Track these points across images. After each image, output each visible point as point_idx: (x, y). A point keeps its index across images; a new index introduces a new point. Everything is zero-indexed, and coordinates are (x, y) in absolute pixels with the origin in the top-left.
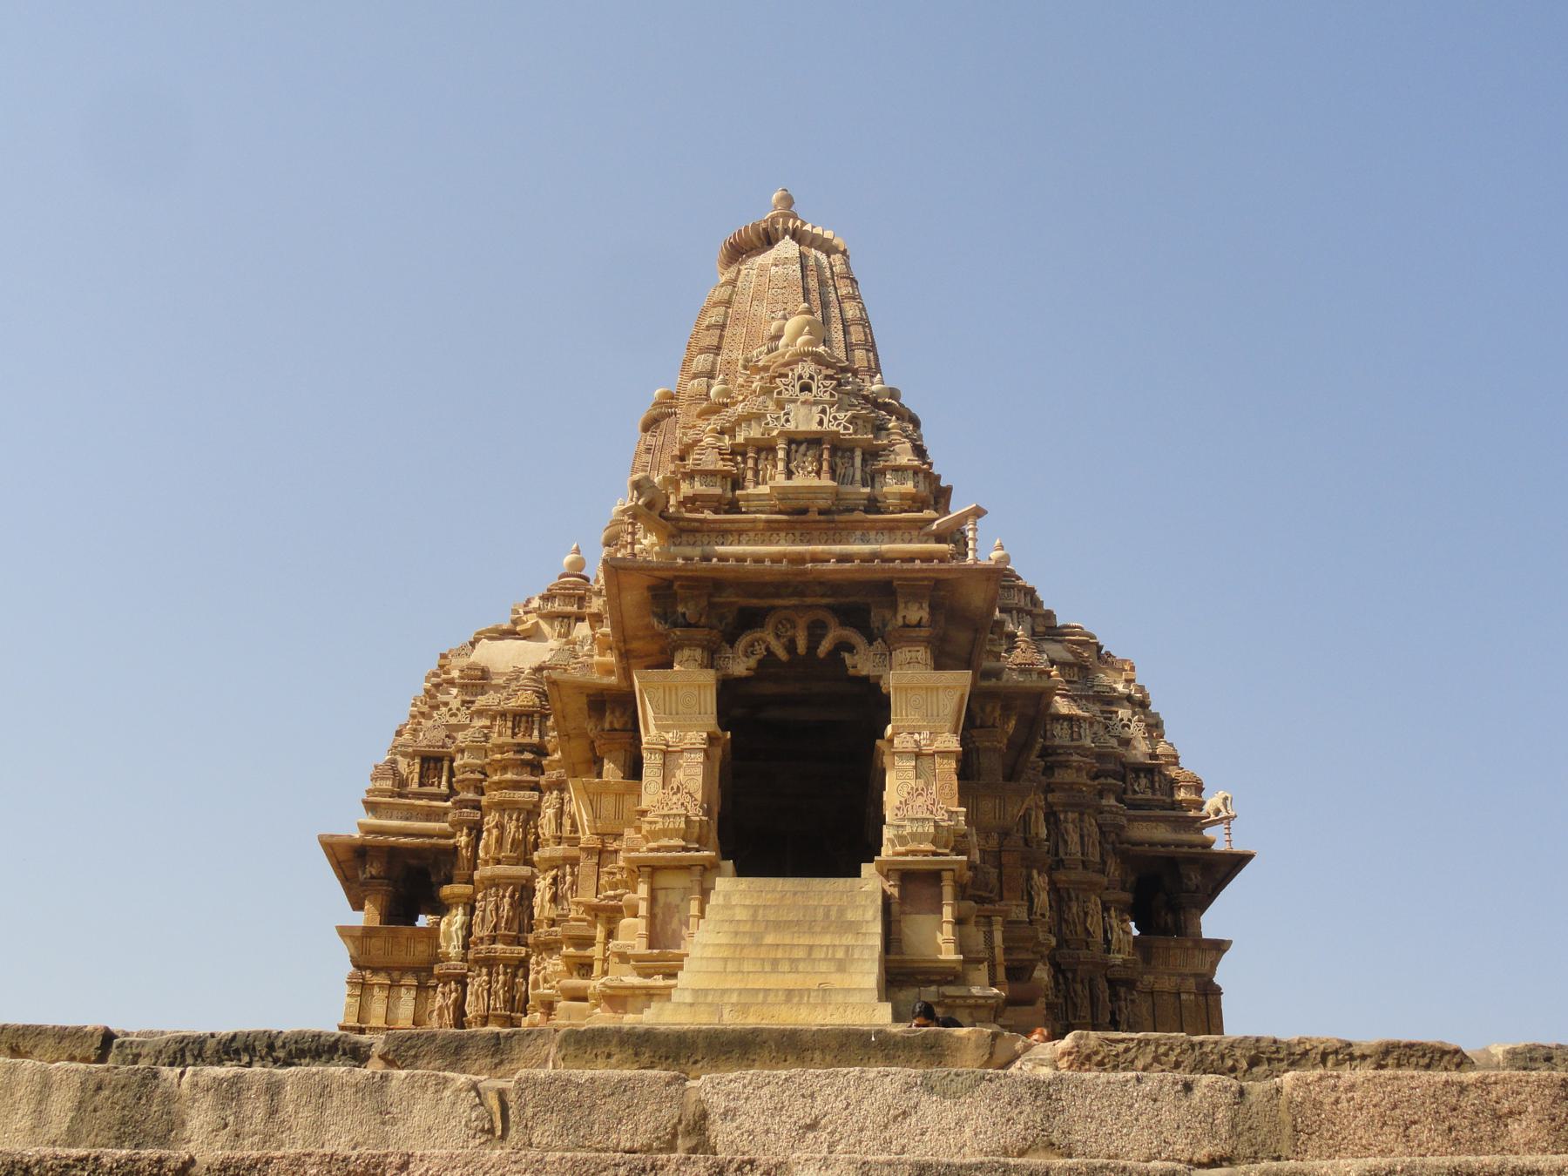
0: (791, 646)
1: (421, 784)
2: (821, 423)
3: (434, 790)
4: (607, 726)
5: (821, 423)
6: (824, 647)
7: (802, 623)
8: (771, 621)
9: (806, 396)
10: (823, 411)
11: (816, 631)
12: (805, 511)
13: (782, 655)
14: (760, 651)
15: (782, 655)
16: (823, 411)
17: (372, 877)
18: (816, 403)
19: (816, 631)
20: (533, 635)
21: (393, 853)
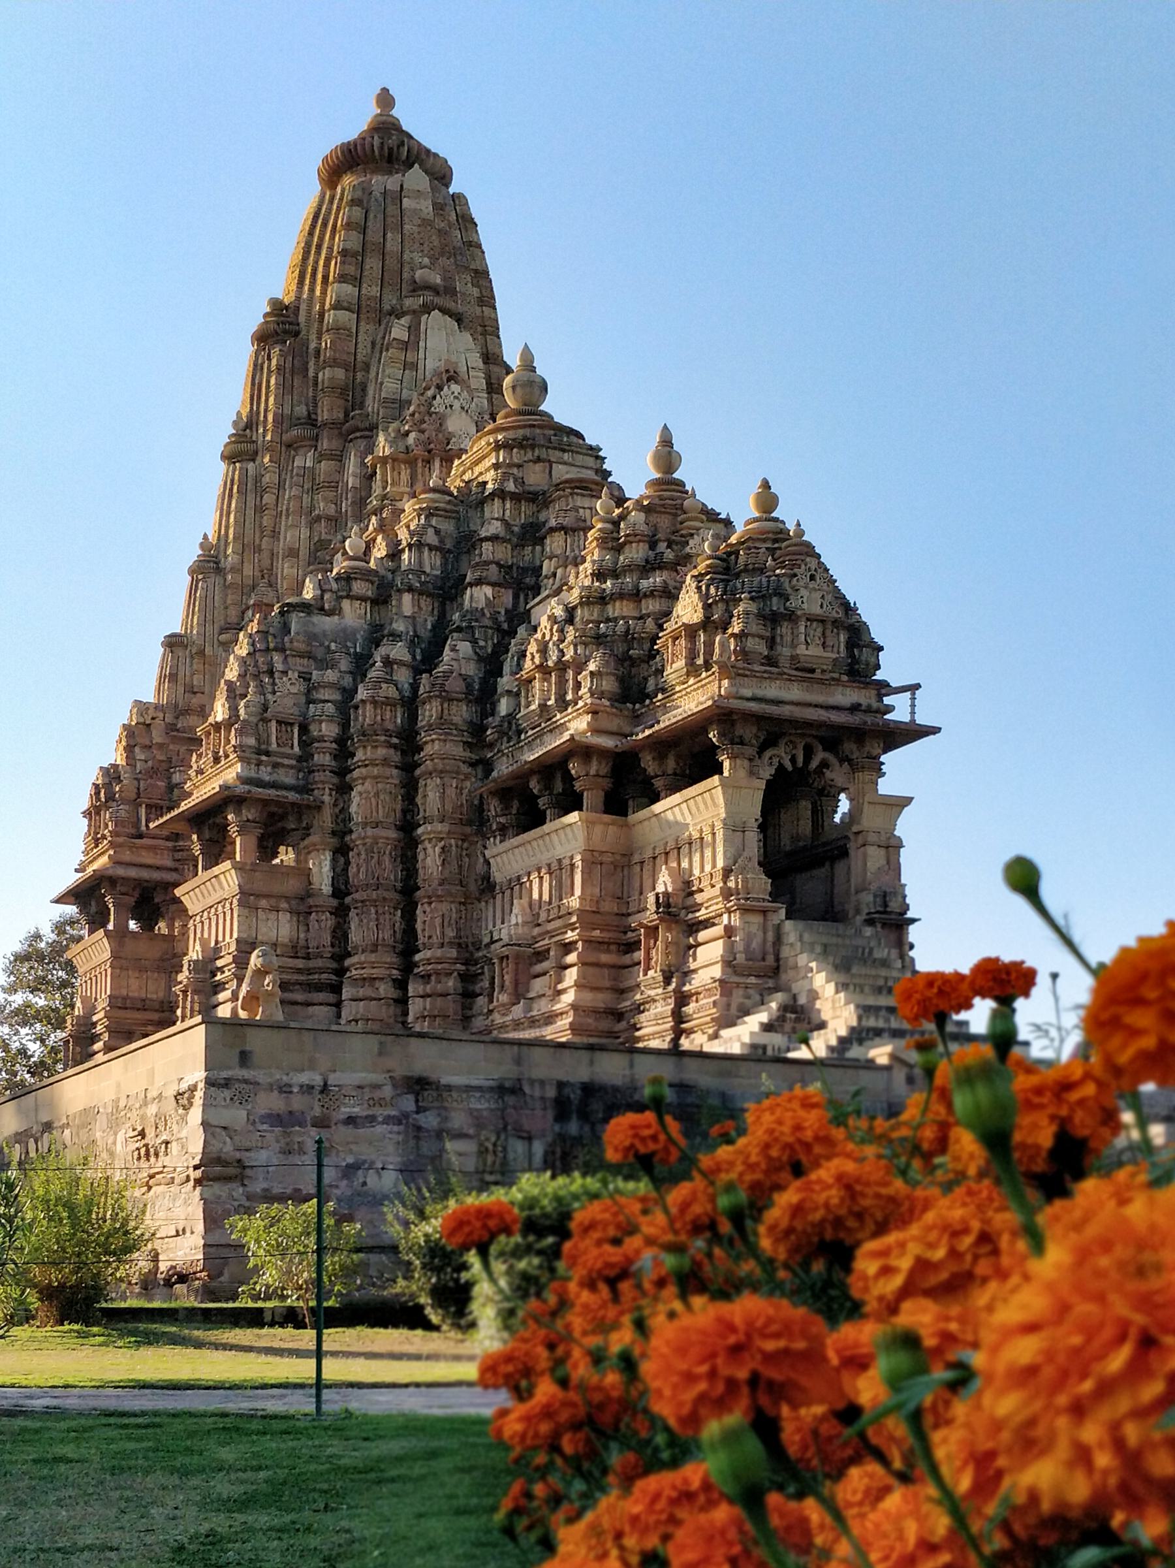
0: (793, 760)
1: (278, 745)
2: (822, 606)
3: (287, 750)
4: (592, 772)
5: (822, 606)
6: (814, 764)
7: (801, 747)
8: (782, 743)
9: (812, 585)
11: (809, 753)
12: (812, 671)
13: (789, 766)
14: (776, 761)
15: (789, 766)
17: (248, 820)
19: (809, 753)
20: (335, 611)
21: (265, 803)
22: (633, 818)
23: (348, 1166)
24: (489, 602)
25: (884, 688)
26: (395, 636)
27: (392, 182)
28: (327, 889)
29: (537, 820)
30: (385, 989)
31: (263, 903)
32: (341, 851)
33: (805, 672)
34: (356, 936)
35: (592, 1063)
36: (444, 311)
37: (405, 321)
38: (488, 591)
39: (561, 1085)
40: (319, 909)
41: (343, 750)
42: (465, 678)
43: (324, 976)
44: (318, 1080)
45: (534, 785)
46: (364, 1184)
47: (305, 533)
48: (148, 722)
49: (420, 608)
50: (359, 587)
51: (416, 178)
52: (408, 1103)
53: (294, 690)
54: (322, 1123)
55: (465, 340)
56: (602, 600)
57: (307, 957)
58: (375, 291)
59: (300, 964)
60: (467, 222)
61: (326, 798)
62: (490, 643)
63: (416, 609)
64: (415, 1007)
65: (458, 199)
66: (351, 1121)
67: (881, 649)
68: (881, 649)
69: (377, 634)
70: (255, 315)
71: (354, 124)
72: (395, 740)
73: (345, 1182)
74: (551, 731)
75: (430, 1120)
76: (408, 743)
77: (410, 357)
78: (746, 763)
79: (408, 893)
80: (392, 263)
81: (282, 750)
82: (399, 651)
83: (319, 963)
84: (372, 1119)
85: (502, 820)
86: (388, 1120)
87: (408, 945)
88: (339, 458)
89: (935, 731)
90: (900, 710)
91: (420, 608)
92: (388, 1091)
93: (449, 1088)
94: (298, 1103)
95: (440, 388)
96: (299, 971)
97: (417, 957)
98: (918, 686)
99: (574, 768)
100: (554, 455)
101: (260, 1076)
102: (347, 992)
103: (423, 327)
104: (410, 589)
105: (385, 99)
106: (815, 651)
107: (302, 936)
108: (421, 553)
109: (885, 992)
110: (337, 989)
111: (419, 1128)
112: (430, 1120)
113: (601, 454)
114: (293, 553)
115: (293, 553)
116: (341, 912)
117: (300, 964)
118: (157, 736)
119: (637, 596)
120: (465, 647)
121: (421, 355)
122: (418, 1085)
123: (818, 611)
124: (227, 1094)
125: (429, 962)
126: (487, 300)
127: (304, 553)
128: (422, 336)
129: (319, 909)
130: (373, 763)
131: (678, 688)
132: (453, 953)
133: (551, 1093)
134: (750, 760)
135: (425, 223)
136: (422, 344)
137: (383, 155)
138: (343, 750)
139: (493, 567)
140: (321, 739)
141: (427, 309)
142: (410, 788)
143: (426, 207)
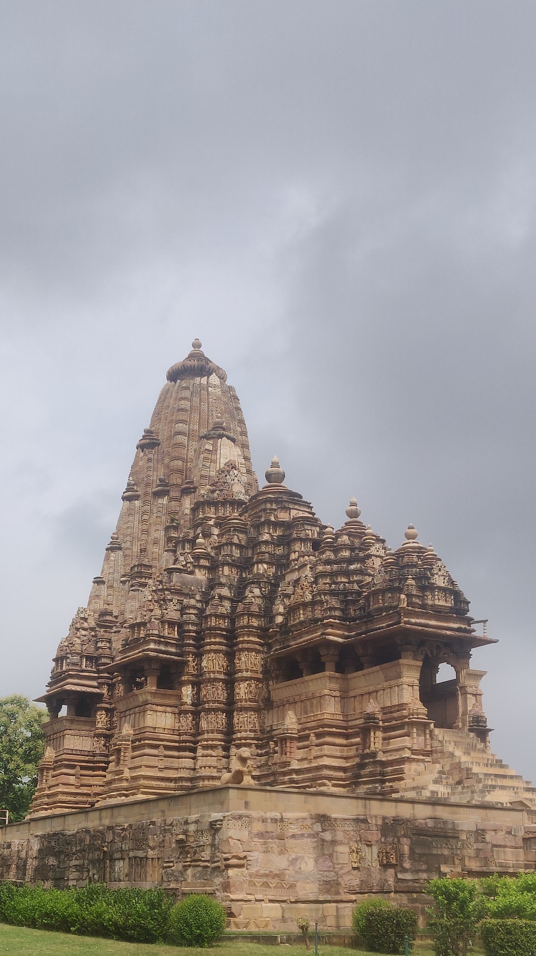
2: (444, 583)
3: (171, 636)
5: (444, 583)
10: (444, 579)
12: (441, 612)
14: (424, 653)
16: (444, 579)
18: (443, 576)
20: (192, 573)
22: (350, 676)
23: (293, 859)
24: (265, 571)
25: (469, 621)
26: (222, 585)
27: (204, 380)
28: (189, 702)
29: (299, 675)
30: (220, 752)
31: (160, 708)
32: (197, 685)
33: (438, 613)
34: (204, 725)
35: (396, 807)
36: (228, 438)
37: (211, 442)
38: (265, 566)
39: (384, 818)
40: (186, 712)
41: (199, 638)
42: (259, 605)
43: (188, 744)
44: (278, 816)
46: (300, 868)
47: (162, 533)
48: (86, 617)
49: (232, 572)
50: (203, 562)
51: (214, 379)
52: (318, 827)
53: (175, 608)
54: (281, 838)
55: (237, 451)
56: (332, 574)
57: (179, 735)
58: (196, 427)
59: (176, 738)
60: (236, 398)
61: (190, 659)
62: (267, 589)
63: (230, 572)
65: (230, 388)
66: (293, 836)
67: (469, 602)
68: (469, 602)
69: (213, 584)
70: (138, 436)
71: (179, 356)
72: (224, 633)
73: (291, 868)
74: (307, 633)
75: (327, 836)
76: (231, 637)
77: (213, 457)
78: (412, 653)
79: (230, 707)
80: (204, 416)
81: (169, 636)
82: (225, 592)
83: (184, 737)
84: (302, 835)
85: (277, 672)
86: (309, 836)
87: (229, 731)
88: (178, 500)
90: (478, 631)
91: (232, 572)
92: (309, 822)
93: (336, 819)
94: (270, 827)
95: (229, 472)
97: (234, 736)
99: (323, 652)
100: (291, 506)
101: (254, 814)
103: (219, 445)
104: (228, 564)
105: (197, 345)
106: (442, 603)
108: (231, 547)
109: (489, 766)
111: (323, 840)
112: (327, 836)
113: (311, 505)
114: (156, 542)
115: (156, 542)
116: (196, 715)
118: (92, 623)
119: (347, 574)
120: (257, 591)
121: (218, 457)
122: (323, 819)
123: (443, 585)
124: (240, 823)
125: (240, 739)
126: (244, 433)
127: (162, 543)
128: (219, 448)
129: (186, 712)
130: (215, 643)
131: (375, 617)
132: (252, 735)
133: (380, 822)
134: (414, 652)
135: (218, 399)
136: (218, 452)
137: (194, 369)
138: (199, 638)
139: (267, 555)
140: (189, 631)
141: (221, 436)
142: (231, 656)
143: (218, 391)
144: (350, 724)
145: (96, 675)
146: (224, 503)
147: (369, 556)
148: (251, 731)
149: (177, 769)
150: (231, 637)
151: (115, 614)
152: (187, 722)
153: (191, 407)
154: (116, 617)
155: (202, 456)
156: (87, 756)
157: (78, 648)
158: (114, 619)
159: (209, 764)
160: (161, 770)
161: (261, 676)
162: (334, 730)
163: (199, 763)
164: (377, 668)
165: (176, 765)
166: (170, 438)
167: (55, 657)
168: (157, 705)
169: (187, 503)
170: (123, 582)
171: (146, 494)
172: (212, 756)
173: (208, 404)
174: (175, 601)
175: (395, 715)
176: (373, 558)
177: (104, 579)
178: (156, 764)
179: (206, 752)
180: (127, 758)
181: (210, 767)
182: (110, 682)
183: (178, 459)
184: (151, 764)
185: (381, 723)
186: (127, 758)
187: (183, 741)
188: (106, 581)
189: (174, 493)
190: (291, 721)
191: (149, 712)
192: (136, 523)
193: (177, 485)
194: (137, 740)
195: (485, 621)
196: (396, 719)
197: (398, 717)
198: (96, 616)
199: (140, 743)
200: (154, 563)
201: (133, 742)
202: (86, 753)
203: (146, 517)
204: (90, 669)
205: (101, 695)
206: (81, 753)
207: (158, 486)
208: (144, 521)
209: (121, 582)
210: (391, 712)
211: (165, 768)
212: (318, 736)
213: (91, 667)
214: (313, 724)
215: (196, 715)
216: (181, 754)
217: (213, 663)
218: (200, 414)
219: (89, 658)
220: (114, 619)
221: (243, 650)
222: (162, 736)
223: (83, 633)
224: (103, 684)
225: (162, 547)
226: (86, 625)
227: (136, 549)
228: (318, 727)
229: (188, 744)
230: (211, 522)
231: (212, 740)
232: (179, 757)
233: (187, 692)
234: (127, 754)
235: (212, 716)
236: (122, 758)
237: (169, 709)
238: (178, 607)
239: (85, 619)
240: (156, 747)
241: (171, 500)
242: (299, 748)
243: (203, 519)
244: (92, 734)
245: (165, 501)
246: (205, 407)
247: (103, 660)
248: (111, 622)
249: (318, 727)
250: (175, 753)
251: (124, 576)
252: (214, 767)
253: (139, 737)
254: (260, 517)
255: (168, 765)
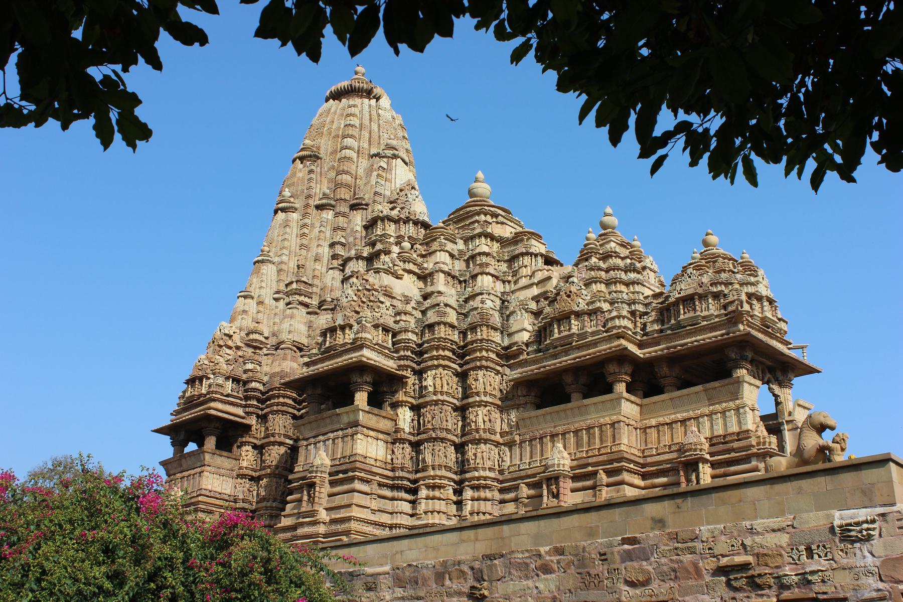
20: (399, 277)
31: (372, 433)
37: (385, 160)
40: (402, 441)
43: (405, 482)
45: (568, 379)
47: (327, 249)
57: (393, 470)
58: (366, 145)
59: (390, 474)
64: (468, 507)
74: (578, 348)
77: (389, 176)
80: (375, 136)
89: (819, 372)
96: (387, 477)
98: (806, 347)
102: (423, 492)
107: (389, 457)
110: (414, 491)
117: (390, 474)
127: (325, 260)
129: (402, 441)
136: (393, 172)
141: (395, 157)
144: (649, 460)
145: (244, 403)
146: (407, 221)
147: (644, 268)
148: (490, 469)
149: (391, 513)
150: (463, 353)
151: (266, 335)
152: (404, 454)
153: (361, 125)
154: (267, 338)
155: (375, 173)
156: (227, 501)
157: (224, 367)
158: (263, 340)
159: (437, 508)
160: (374, 511)
161: (499, 403)
162: (632, 466)
163: (422, 506)
164: (699, 388)
165: (390, 509)
166: (334, 152)
167: (188, 377)
168: (368, 428)
169: (358, 219)
170: (276, 300)
171: (307, 206)
172: (439, 499)
173: (379, 125)
174: (388, 304)
175: (736, 445)
176: (648, 271)
177: (252, 294)
178: (368, 504)
179: (431, 493)
180: (322, 495)
181: (439, 512)
182: (260, 412)
183: (347, 173)
184: (363, 503)
185: (708, 457)
186: (322, 495)
187: (399, 478)
188: (256, 296)
189: (344, 208)
190: (561, 457)
191: (359, 436)
192: (294, 236)
193: (345, 200)
194: (338, 473)
195: (802, 348)
196: (733, 450)
197: (740, 448)
198: (243, 334)
199: (346, 476)
200: (316, 282)
201: (330, 474)
202: (226, 497)
203: (306, 231)
204: (235, 394)
205: (249, 427)
206: (219, 496)
207: (321, 199)
208: (304, 235)
209: (274, 299)
210: (726, 443)
211: (379, 511)
212: (609, 473)
213: (238, 392)
214: (601, 458)
215: (416, 446)
216: (396, 494)
217: (441, 381)
218: (370, 134)
219: (236, 380)
220: (263, 340)
221: (480, 368)
222: (375, 470)
223: (228, 351)
224: (252, 413)
225: (325, 264)
226: (230, 343)
227: (292, 264)
228: (611, 462)
229: (405, 482)
230: (392, 240)
231: (441, 477)
232: (393, 499)
233: (405, 416)
234: (323, 490)
235: (439, 446)
236: (317, 494)
237: (381, 436)
238: (391, 312)
239: (230, 337)
240: (368, 482)
241: (337, 215)
242: (573, 491)
243: (381, 236)
244: (235, 474)
245: (329, 215)
246: (375, 127)
247: (254, 385)
248: (262, 342)
249: (611, 462)
250: (388, 493)
251: (277, 292)
252: (444, 513)
253: (344, 467)
254: (474, 229)
255: (383, 507)
